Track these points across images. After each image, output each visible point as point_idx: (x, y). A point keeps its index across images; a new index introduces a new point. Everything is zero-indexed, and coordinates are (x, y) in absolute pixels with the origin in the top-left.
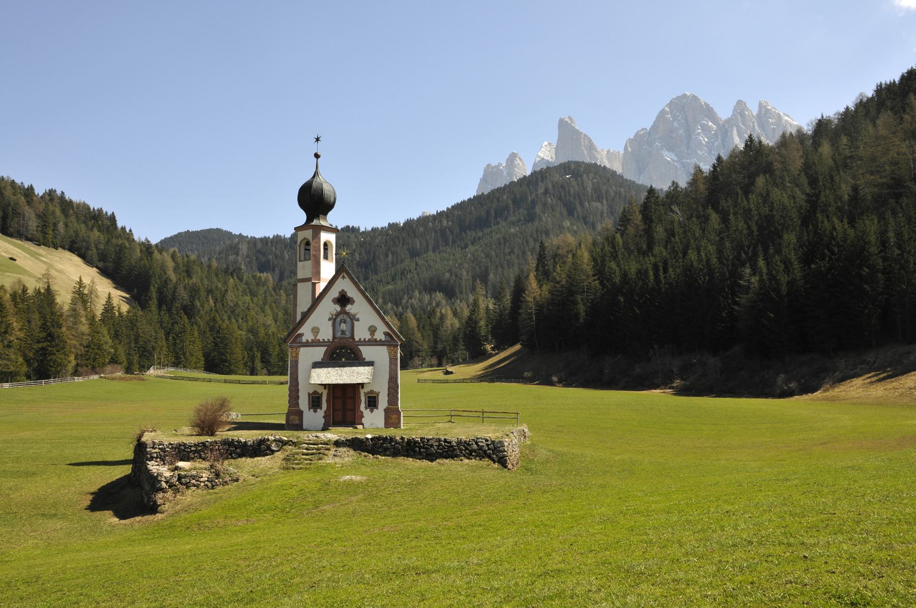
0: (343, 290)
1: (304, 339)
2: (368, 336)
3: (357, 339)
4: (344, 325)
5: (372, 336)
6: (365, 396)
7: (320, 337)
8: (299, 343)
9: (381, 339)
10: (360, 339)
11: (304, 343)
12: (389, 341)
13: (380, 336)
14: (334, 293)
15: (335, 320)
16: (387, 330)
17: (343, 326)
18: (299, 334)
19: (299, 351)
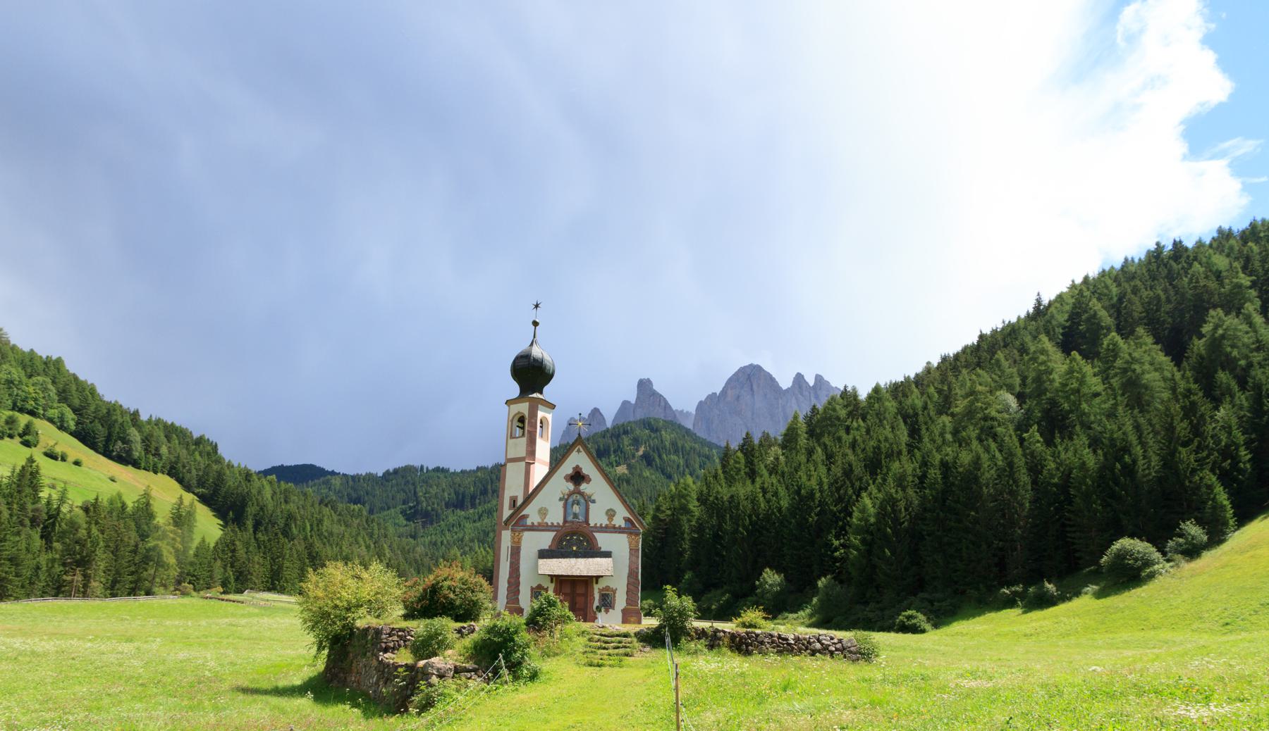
0: (577, 466)
1: (529, 522)
2: (605, 522)
3: (592, 524)
4: (577, 507)
6: (600, 592)
7: (549, 520)
9: (620, 526)
12: (629, 529)
13: (619, 521)
14: (567, 468)
15: (567, 500)
16: (628, 515)
17: (576, 509)
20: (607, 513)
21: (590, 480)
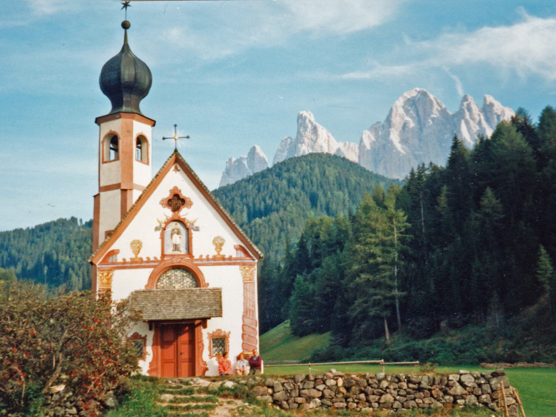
0: (176, 188)
1: (119, 258)
2: (212, 252)
7: (143, 255)
8: (113, 263)
10: (201, 256)
11: (120, 263)
16: (239, 243)
19: (111, 276)
20: (214, 242)
21: (191, 204)
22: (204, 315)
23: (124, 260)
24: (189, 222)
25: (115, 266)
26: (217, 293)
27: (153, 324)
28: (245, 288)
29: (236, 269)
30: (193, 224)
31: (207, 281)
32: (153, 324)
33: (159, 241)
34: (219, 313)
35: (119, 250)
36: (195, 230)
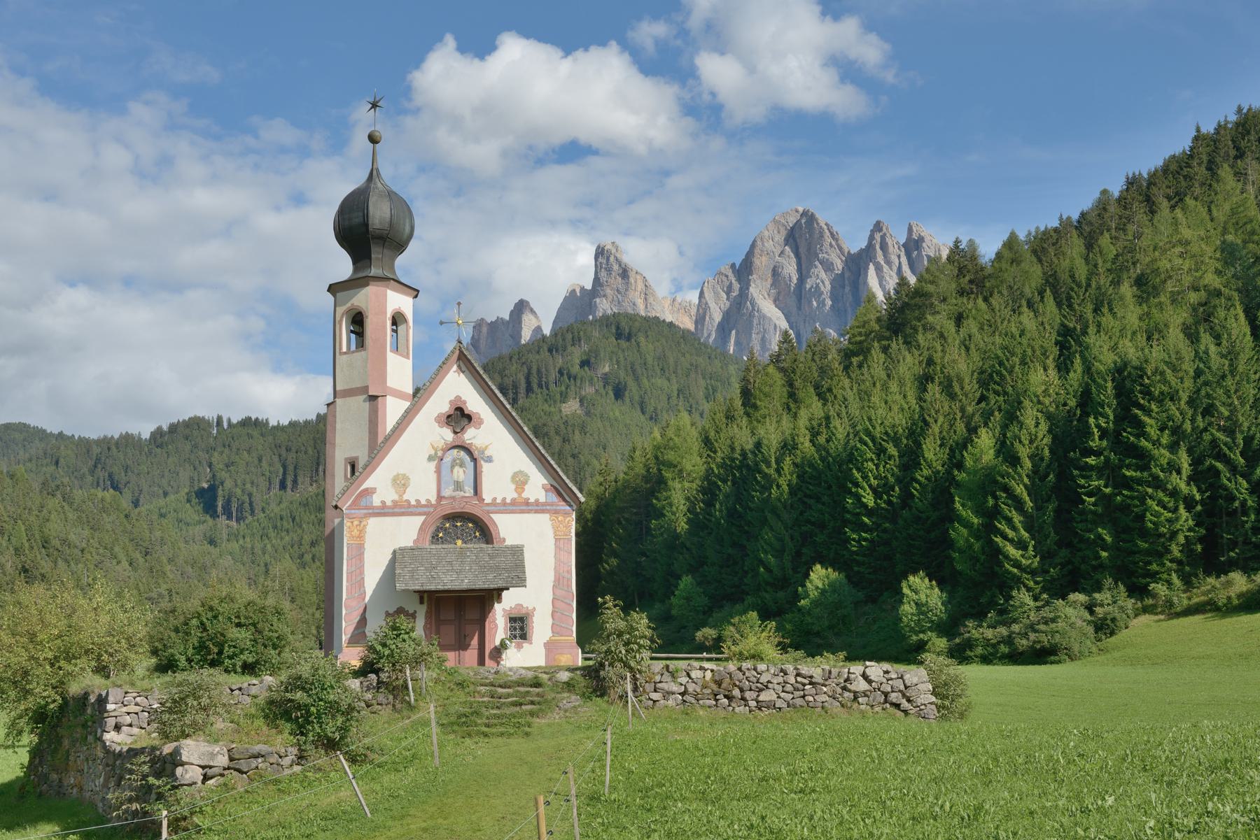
2: (510, 494)
3: (488, 499)
4: (461, 470)
5: (520, 494)
7: (411, 496)
8: (367, 508)
9: (537, 501)
10: (495, 499)
11: (377, 508)
14: (439, 403)
17: (459, 474)
18: (366, 490)
22: (500, 584)
23: (383, 502)
24: (477, 448)
25: (371, 511)
26: (517, 552)
27: (426, 595)
28: (557, 547)
29: (545, 518)
30: (483, 453)
31: (502, 536)
32: (426, 595)
33: (433, 477)
34: (521, 582)
35: (376, 488)
36: (487, 461)
